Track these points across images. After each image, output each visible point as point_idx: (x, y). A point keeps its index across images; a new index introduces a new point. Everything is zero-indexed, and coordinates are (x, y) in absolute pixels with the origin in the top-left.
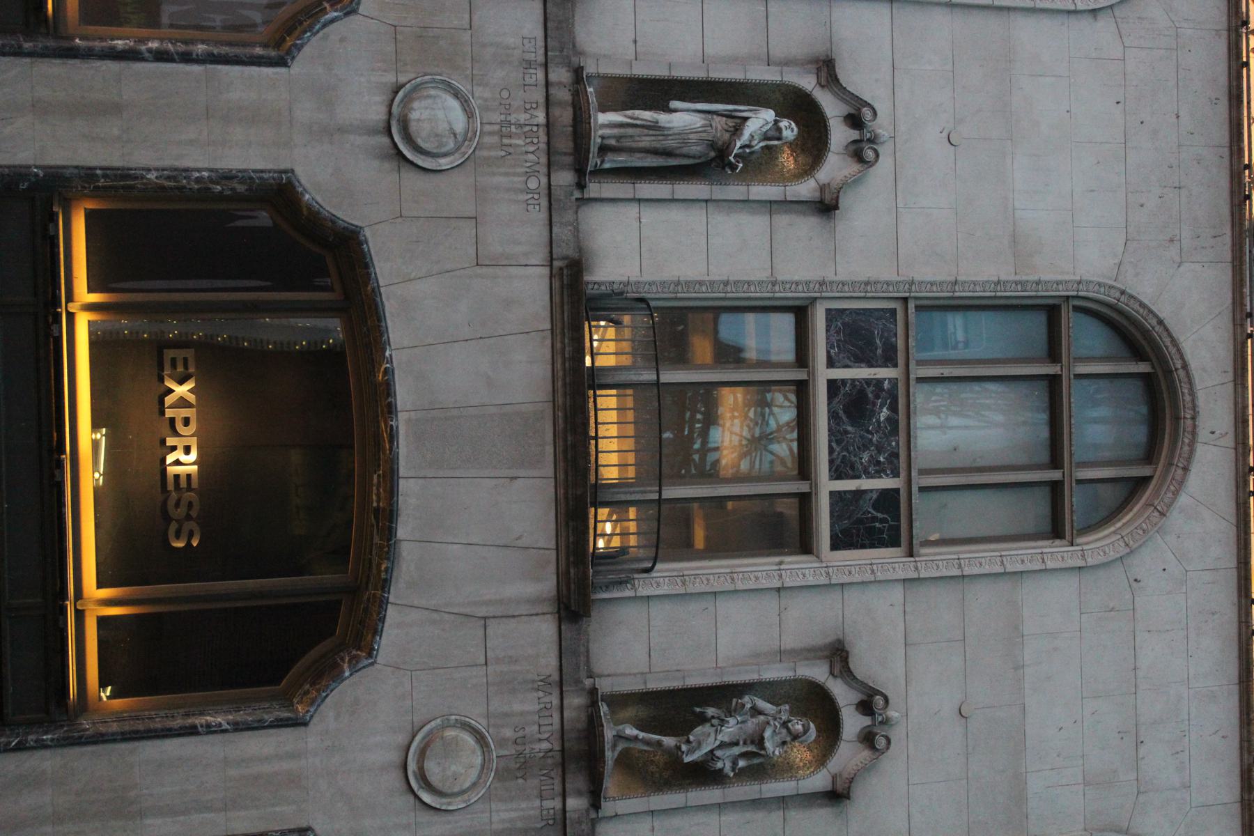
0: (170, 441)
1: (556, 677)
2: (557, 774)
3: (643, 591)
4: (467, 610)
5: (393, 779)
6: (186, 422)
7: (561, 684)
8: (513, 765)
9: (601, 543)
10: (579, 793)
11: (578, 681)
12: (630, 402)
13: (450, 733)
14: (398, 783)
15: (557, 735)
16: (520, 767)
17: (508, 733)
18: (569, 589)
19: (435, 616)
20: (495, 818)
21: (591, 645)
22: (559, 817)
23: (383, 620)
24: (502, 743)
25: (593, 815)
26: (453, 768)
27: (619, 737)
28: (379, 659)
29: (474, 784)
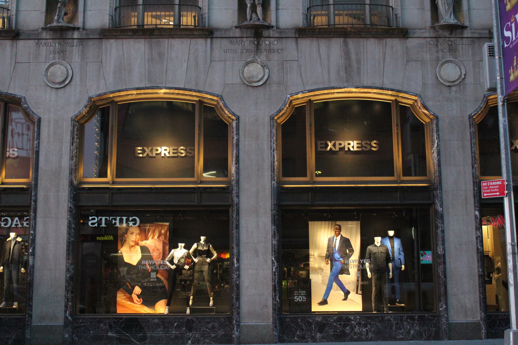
0: (163, 155)
1: (36, 41)
2: (66, 41)
3: (14, 12)
4: (12, 69)
5: (61, 92)
6: (157, 150)
7: (38, 39)
8: (62, 54)
9: (172, 23)
10: (73, 34)
11: (38, 34)
12: (185, 13)
13: (49, 74)
14: (63, 90)
15: (55, 40)
16: (62, 52)
17: (52, 56)
18: (8, 36)
19: (13, 78)
20: (77, 60)
21: (30, 29)
22: (80, 40)
23: (11, 94)
24: (54, 58)
25: (275, 28)
26: (59, 73)
27: (58, 21)
28: (24, 96)
29: (66, 67)
